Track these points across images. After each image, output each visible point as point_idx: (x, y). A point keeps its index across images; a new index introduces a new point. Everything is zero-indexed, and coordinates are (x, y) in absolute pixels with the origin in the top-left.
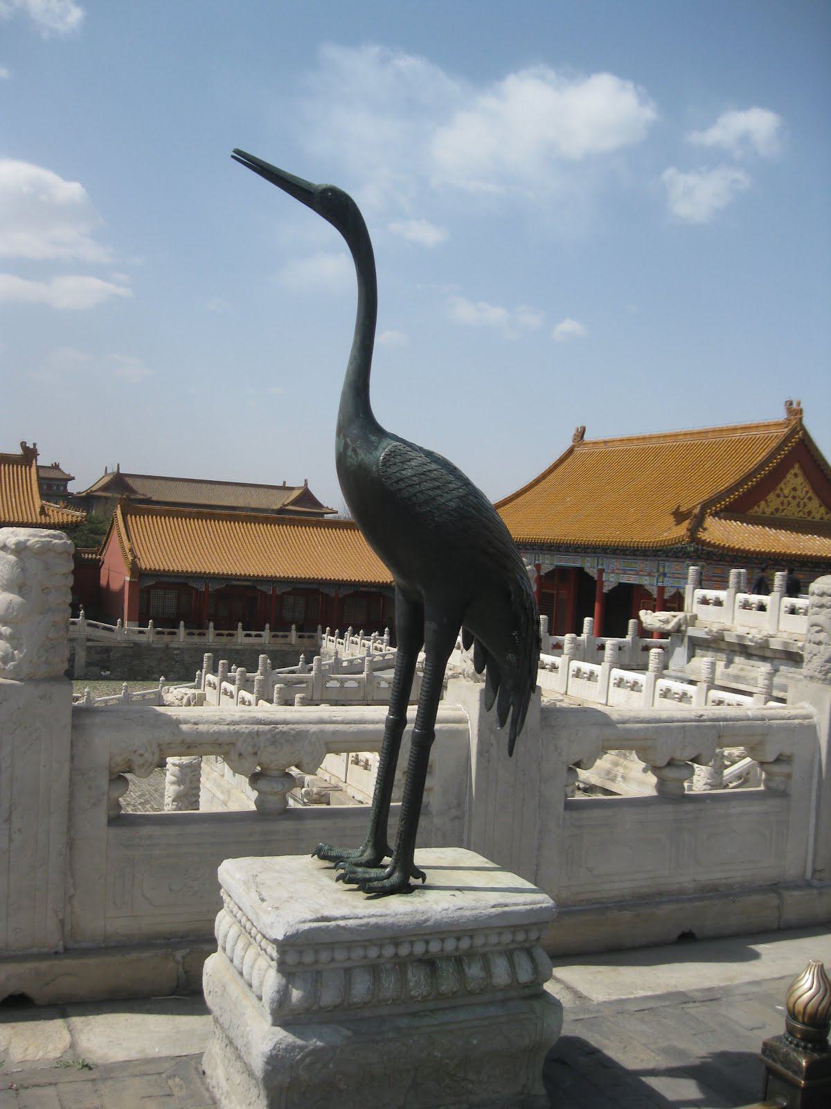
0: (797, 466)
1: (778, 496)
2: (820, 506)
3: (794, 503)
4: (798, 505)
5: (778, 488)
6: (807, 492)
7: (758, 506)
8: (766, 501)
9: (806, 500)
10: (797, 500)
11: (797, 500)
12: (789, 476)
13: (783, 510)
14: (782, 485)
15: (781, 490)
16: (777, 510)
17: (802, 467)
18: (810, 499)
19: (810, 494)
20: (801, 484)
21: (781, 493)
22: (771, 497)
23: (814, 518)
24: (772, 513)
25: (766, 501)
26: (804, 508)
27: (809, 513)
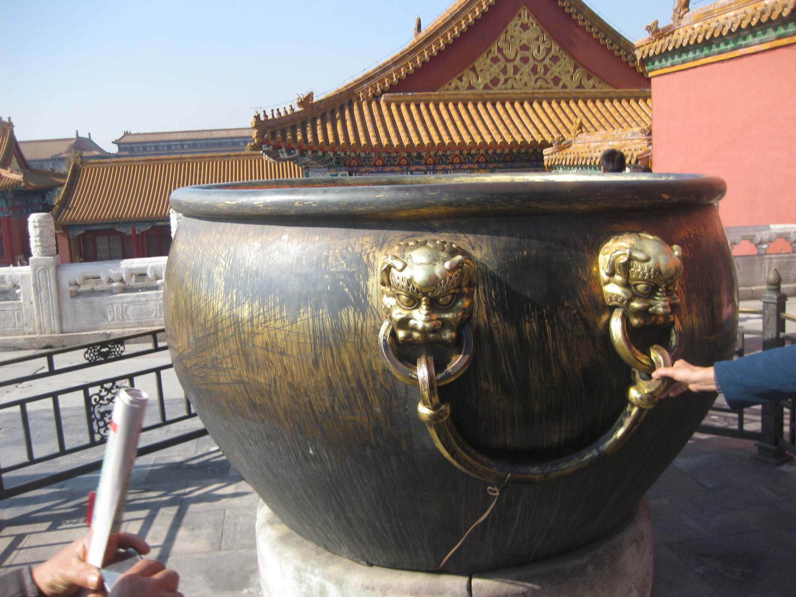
0: (524, 12)
1: (495, 60)
2: (575, 68)
3: (526, 68)
4: (534, 70)
5: (494, 48)
6: (549, 50)
7: (460, 79)
8: (473, 69)
9: (547, 61)
10: (531, 63)
11: (531, 63)
12: (513, 28)
13: (506, 81)
14: (501, 44)
15: (500, 50)
16: (495, 81)
17: (533, 13)
18: (555, 59)
19: (555, 49)
20: (537, 39)
21: (500, 56)
22: (482, 62)
23: (564, 87)
24: (486, 87)
25: (473, 69)
26: (545, 73)
27: (556, 80)
